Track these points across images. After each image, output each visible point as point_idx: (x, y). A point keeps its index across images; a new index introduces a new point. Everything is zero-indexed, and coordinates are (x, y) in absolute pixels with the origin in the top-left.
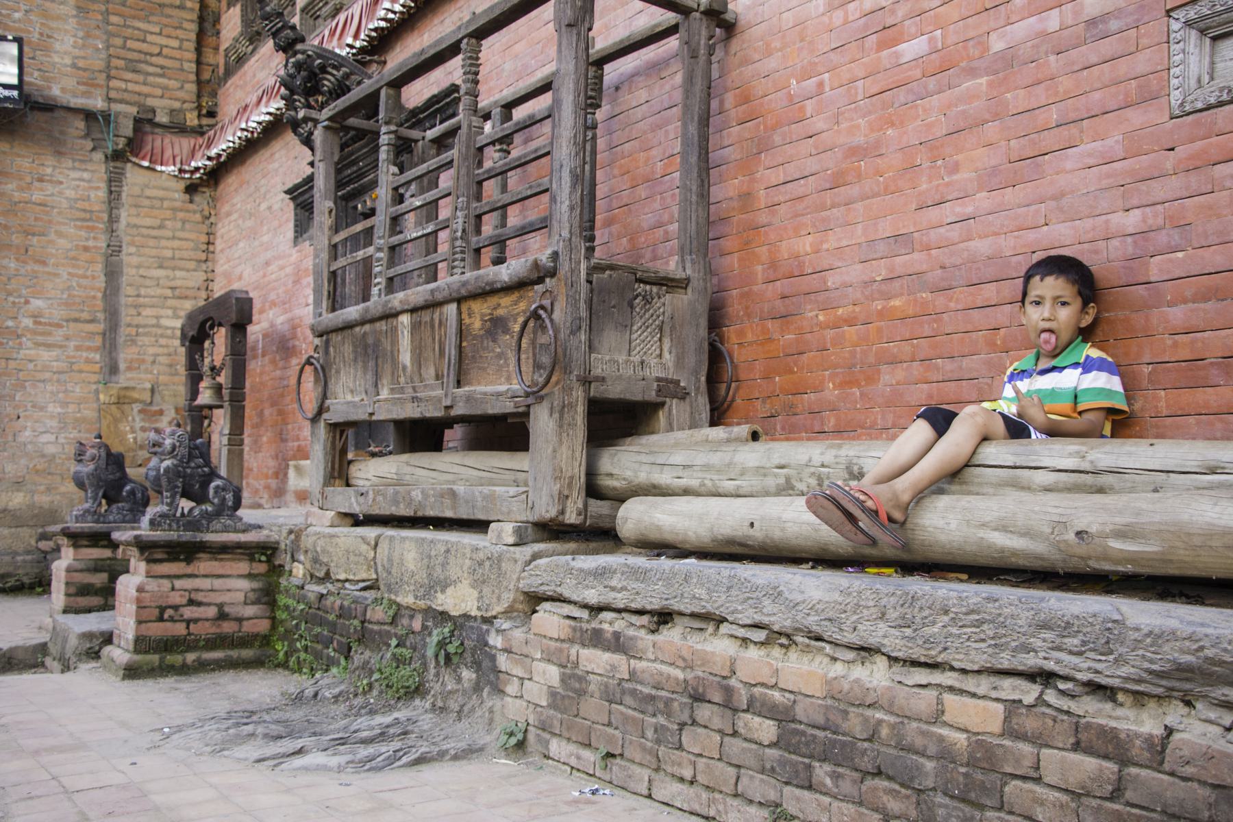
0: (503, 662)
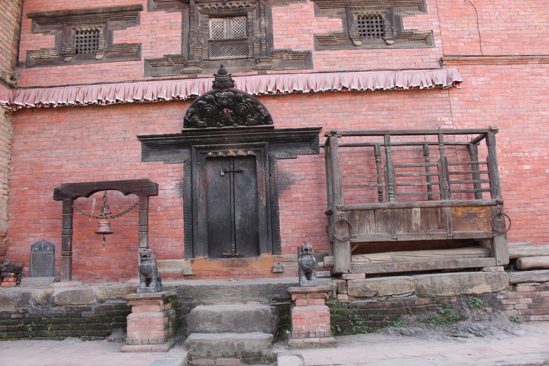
0: (504, 302)
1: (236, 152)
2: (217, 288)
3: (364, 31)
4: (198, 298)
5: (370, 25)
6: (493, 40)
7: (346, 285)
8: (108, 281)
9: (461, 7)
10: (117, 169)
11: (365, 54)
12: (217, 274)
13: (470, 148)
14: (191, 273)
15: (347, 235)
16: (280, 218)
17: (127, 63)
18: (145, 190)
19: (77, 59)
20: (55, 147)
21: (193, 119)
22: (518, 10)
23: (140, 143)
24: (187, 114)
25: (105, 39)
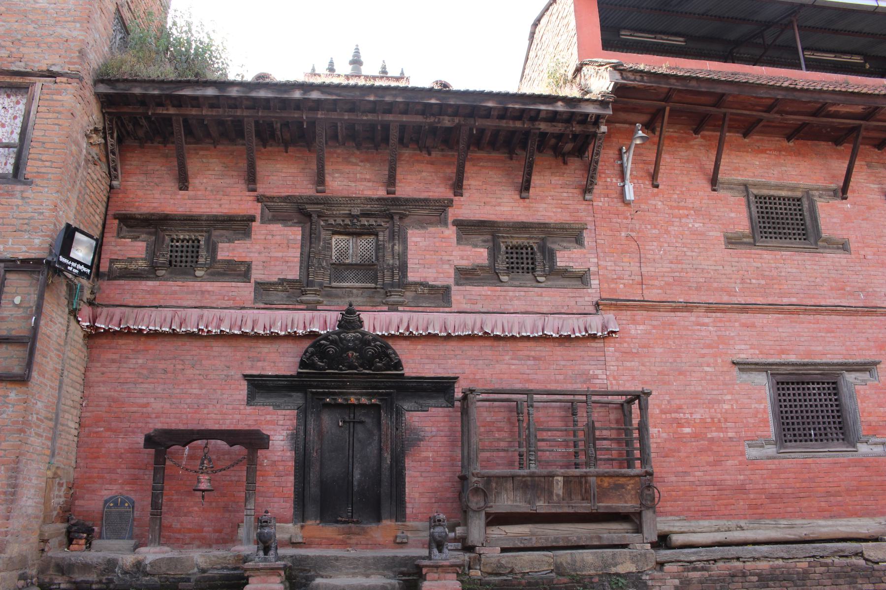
0: (650, 583)
1: (359, 400)
2: (337, 559)
3: (512, 263)
4: (315, 570)
5: (519, 256)
6: (656, 283)
7: (480, 560)
8: (199, 547)
9: (623, 242)
10: (216, 412)
11: (511, 292)
12: (331, 543)
13: (624, 409)
14: (300, 540)
15: (482, 504)
16: (407, 480)
17: (233, 284)
18: (253, 441)
19: (171, 273)
20: (140, 380)
21: (313, 360)
22: (685, 249)
23: (246, 382)
24: (305, 354)
25: (208, 252)
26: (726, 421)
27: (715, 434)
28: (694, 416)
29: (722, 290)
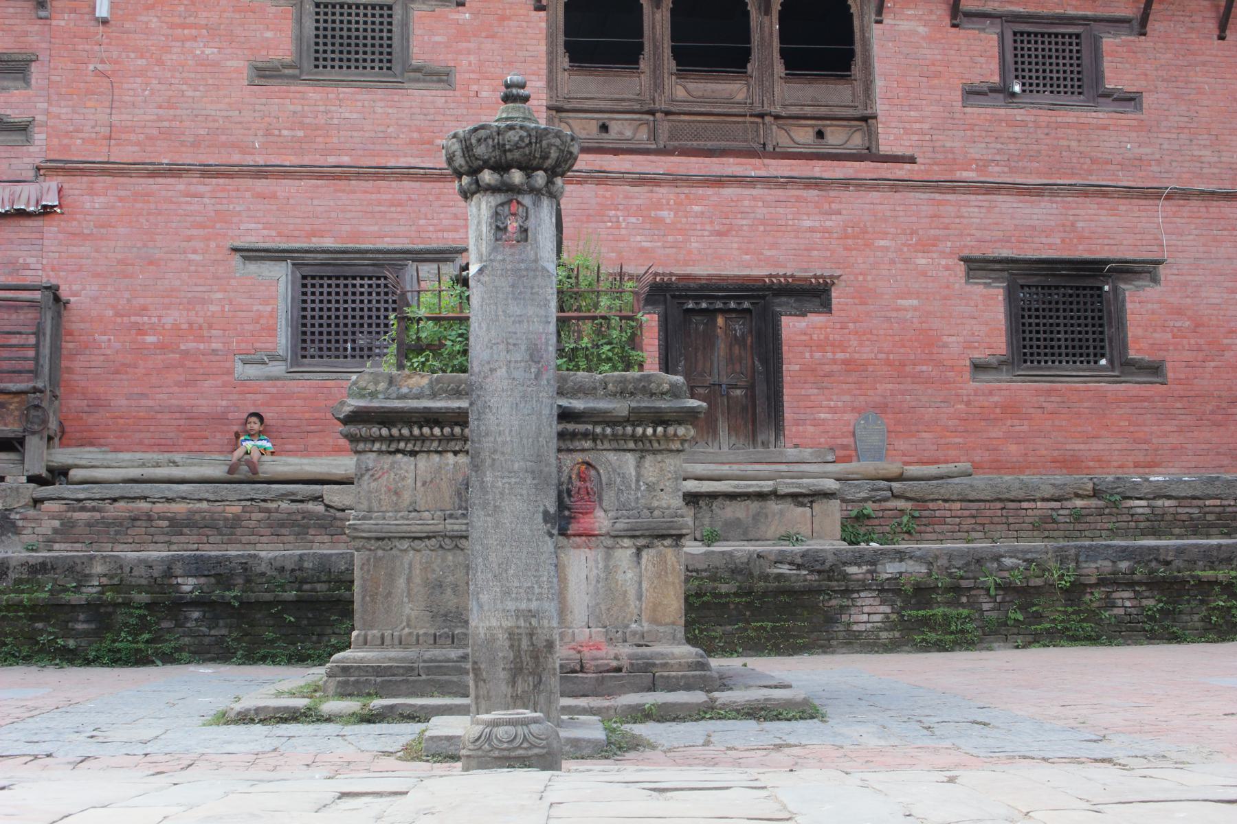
0: (20, 523)
6: (133, 137)
9: (88, 79)
26: (210, 327)
27: (192, 345)
28: (164, 321)
29: (234, 146)
